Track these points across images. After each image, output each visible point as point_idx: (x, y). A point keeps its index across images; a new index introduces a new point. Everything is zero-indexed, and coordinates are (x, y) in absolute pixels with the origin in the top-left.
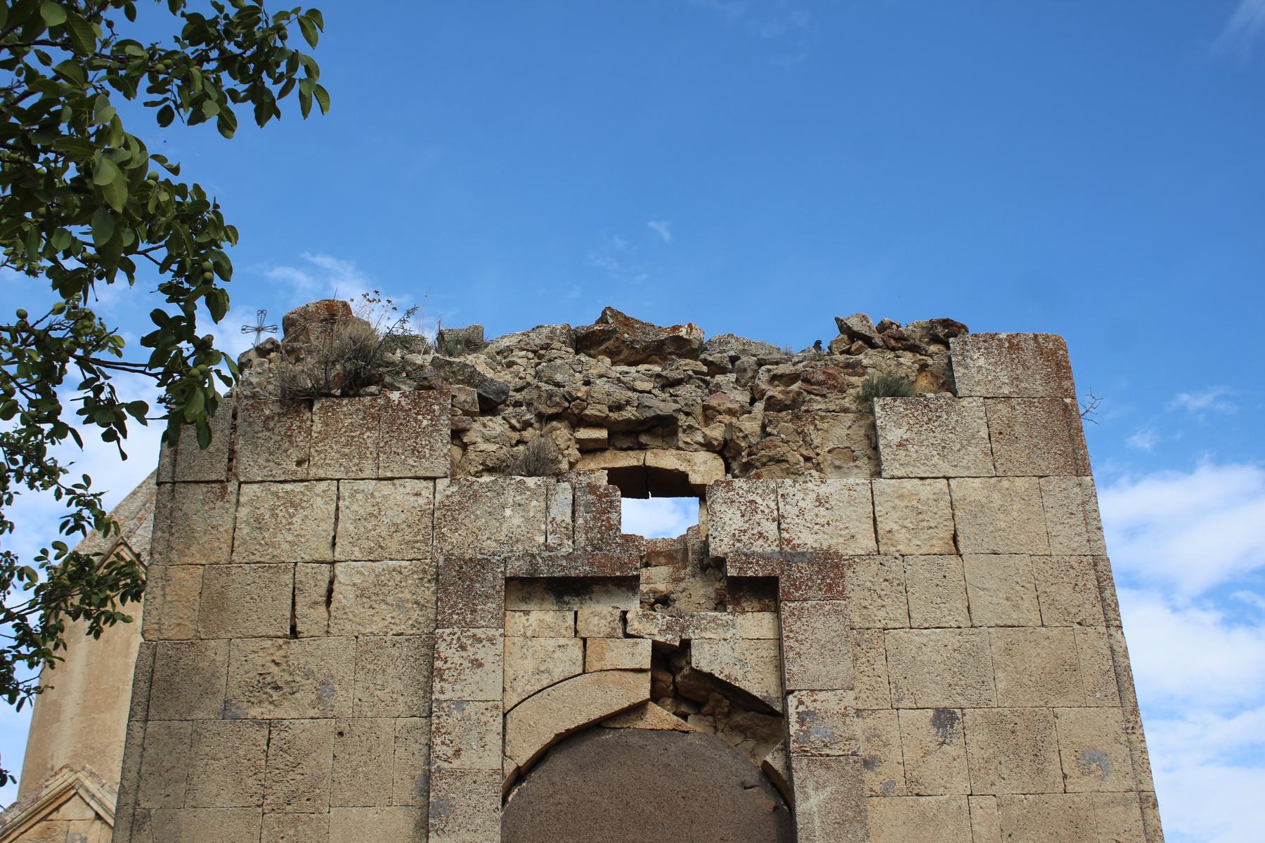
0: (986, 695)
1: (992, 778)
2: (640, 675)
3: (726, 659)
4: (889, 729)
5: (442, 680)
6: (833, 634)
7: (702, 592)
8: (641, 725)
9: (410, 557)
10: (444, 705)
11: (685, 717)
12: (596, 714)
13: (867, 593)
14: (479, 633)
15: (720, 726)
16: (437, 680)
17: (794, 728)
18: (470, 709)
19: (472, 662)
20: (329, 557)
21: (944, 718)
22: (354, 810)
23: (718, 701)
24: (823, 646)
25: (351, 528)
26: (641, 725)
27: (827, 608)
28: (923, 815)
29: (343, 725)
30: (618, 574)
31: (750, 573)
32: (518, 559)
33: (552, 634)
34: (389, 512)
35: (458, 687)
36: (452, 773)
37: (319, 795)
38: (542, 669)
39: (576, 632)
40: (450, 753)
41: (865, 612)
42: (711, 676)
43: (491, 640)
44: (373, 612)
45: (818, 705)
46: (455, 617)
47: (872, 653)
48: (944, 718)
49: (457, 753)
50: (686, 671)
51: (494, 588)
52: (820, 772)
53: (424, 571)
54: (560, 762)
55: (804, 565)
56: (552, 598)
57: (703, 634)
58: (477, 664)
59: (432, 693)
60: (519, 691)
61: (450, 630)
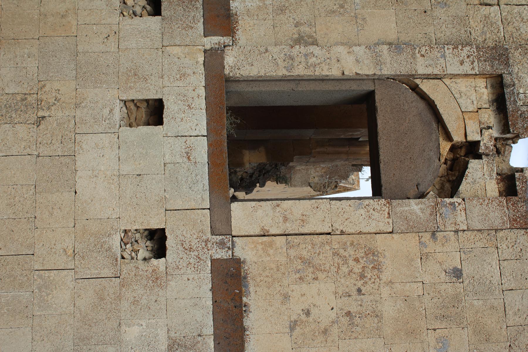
0: (470, 294)
1: (432, 294)
2: (464, 136)
3: (475, 175)
4: (450, 247)
5: (453, 49)
6: (493, 220)
7: (504, 167)
8: (441, 139)
9: (505, 36)
10: (443, 50)
11: (445, 163)
12: (445, 117)
13: (514, 240)
14: (476, 63)
15: (442, 179)
16: (453, 47)
17: (448, 200)
18: (442, 60)
19: (463, 61)
20: (500, 3)
21: (457, 273)
22: (394, 19)
23: (454, 175)
24: (486, 216)
25: (515, 11)
26: (441, 139)
27: (505, 218)
28: (412, 260)
29: (429, 12)
30: (510, 123)
31: (517, 183)
32: (511, 79)
33: (478, 98)
34: (525, 26)
35: (451, 55)
36: (414, 54)
37: (399, 5)
38: (462, 94)
39: (480, 109)
40: (422, 53)
41: (505, 239)
42: (467, 168)
43: (473, 68)
44: (479, 22)
45: (459, 212)
46: (482, 53)
47: (485, 241)
48: (457, 273)
49: (423, 56)
50: (467, 159)
51: (497, 69)
52: (429, 211)
53: (500, 42)
54: (421, 105)
55: (525, 209)
56: (494, 98)
57: (485, 165)
58: (462, 63)
59: (447, 45)
60: (451, 85)
61: (475, 50)
